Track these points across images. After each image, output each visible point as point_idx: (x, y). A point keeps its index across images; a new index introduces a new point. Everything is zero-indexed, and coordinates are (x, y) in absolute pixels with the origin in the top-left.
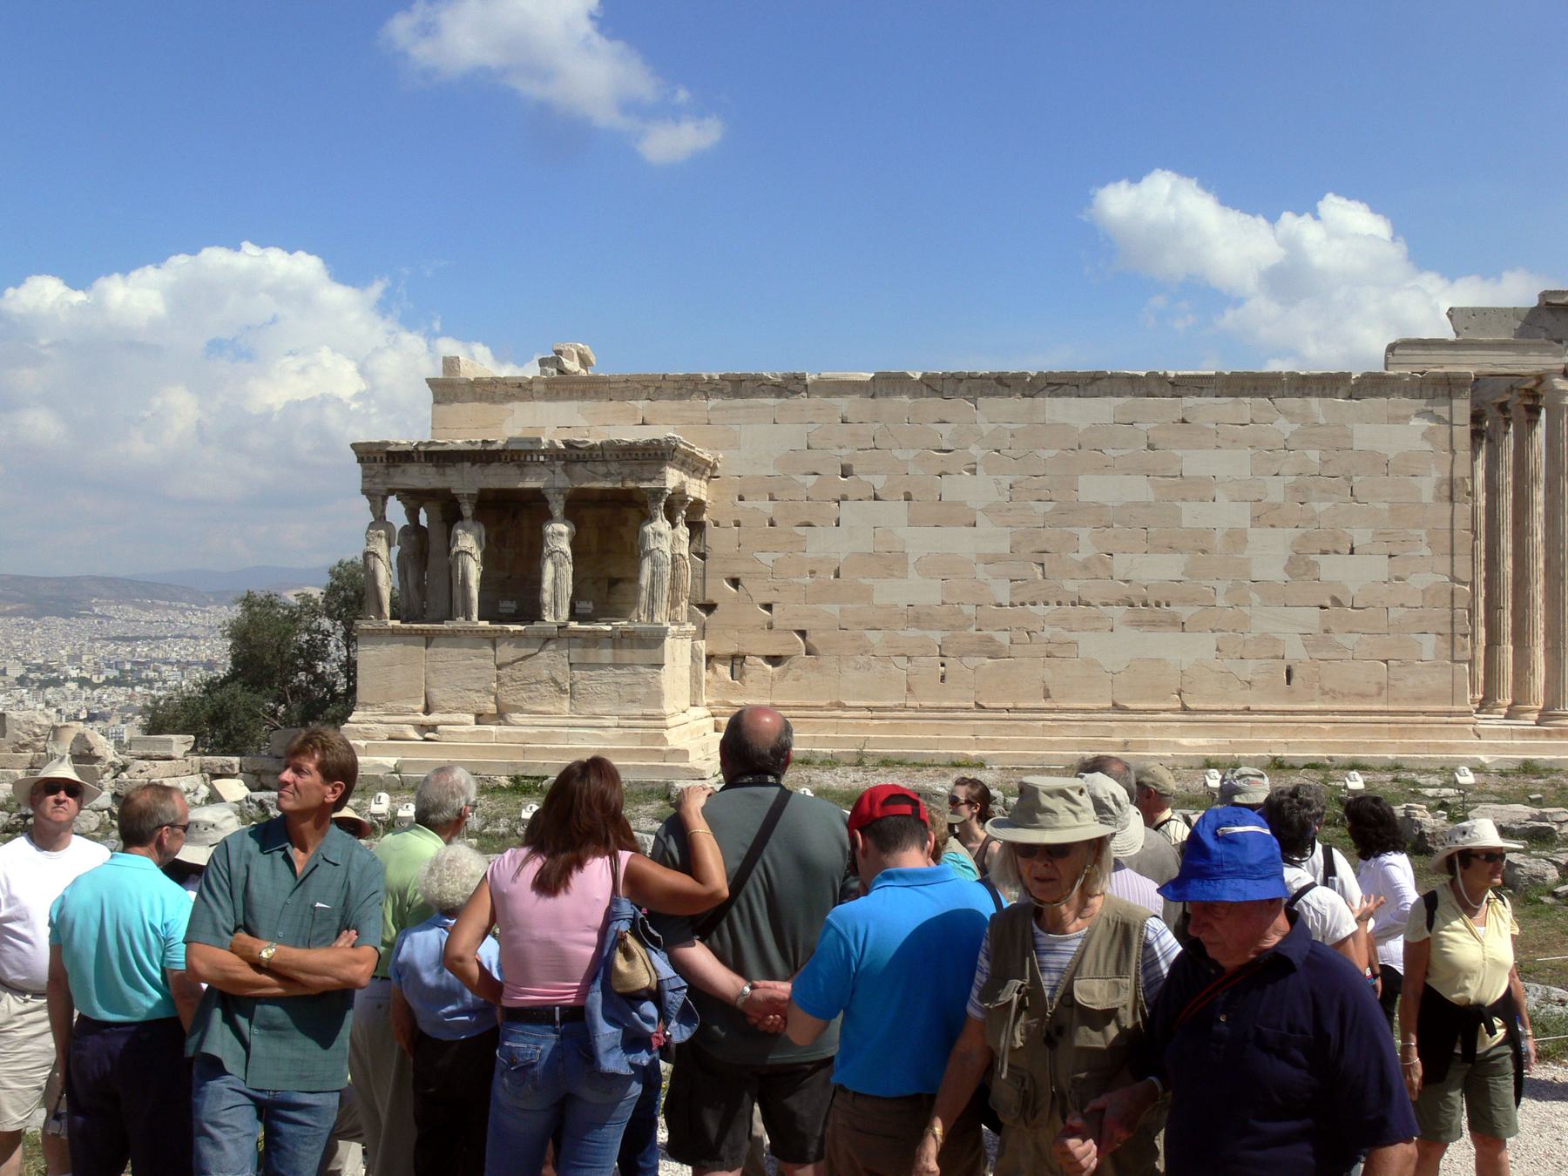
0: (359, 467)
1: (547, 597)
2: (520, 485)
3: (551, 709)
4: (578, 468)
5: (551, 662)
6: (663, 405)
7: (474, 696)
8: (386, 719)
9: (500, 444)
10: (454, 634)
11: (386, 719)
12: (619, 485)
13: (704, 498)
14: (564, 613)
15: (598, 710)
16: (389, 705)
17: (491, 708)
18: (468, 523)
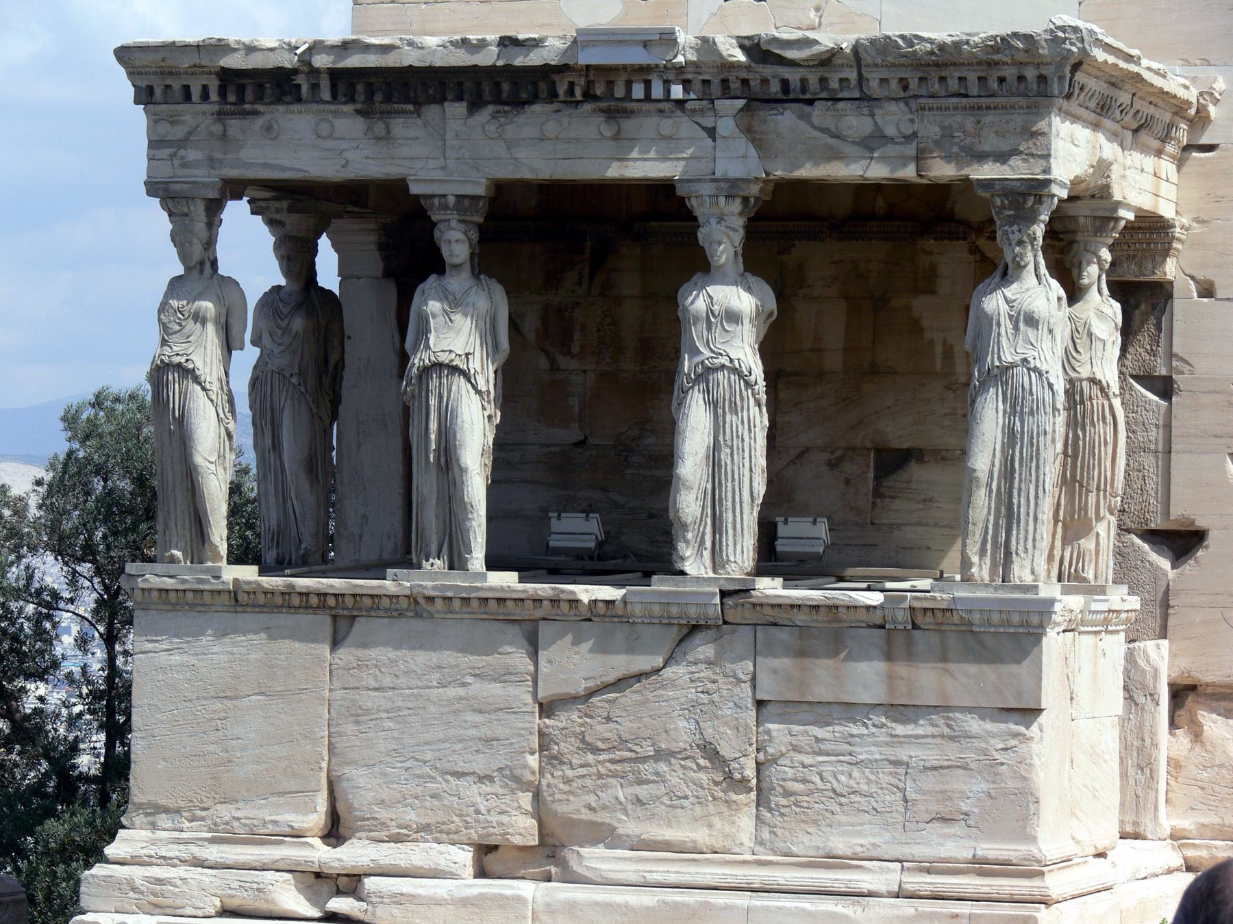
0: (138, 116)
1: (689, 504)
2: (614, 172)
3: (701, 836)
4: (786, 120)
5: (700, 696)
7: (473, 792)
8: (213, 853)
9: (552, 51)
10: (415, 606)
11: (213, 853)
12: (908, 173)
13: (1167, 211)
14: (742, 552)
15: (840, 844)
16: (224, 812)
17: (522, 828)
18: (458, 282)
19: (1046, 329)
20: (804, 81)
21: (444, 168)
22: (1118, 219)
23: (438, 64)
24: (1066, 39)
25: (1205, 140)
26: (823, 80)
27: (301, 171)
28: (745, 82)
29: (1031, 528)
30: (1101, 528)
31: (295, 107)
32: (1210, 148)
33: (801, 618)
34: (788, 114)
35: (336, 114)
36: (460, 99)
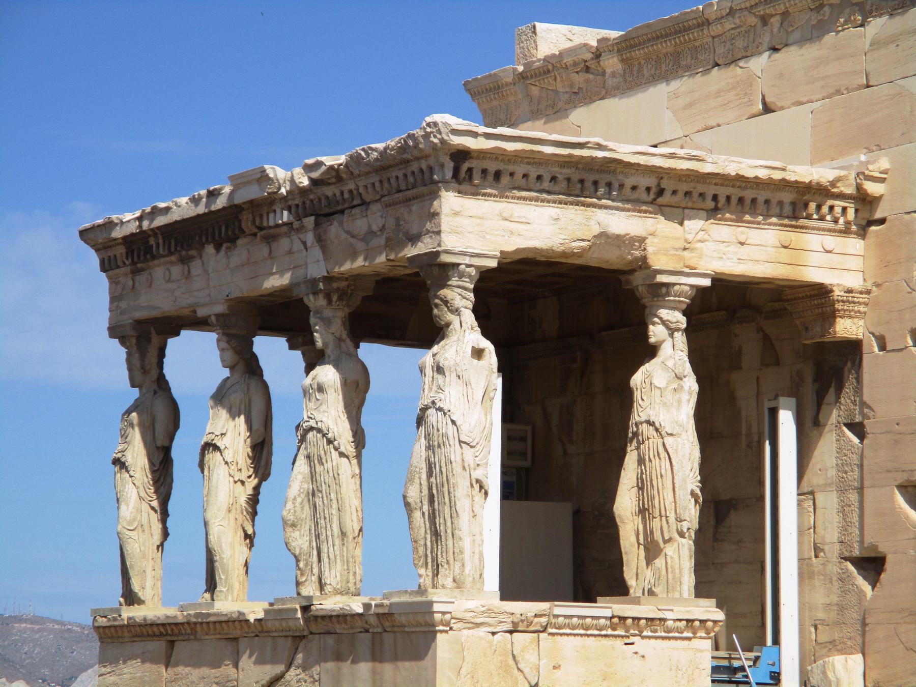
4: (334, 230)
6: (795, 58)
19: (454, 375)
20: (335, 195)
21: (209, 295)
22: (668, 285)
23: (185, 217)
24: (432, 132)
25: (878, 215)
26: (342, 193)
27: (159, 308)
28: (312, 201)
29: (450, 542)
30: (669, 550)
31: (156, 262)
32: (882, 221)
33: (338, 628)
34: (335, 223)
35: (171, 263)
36: (207, 242)
